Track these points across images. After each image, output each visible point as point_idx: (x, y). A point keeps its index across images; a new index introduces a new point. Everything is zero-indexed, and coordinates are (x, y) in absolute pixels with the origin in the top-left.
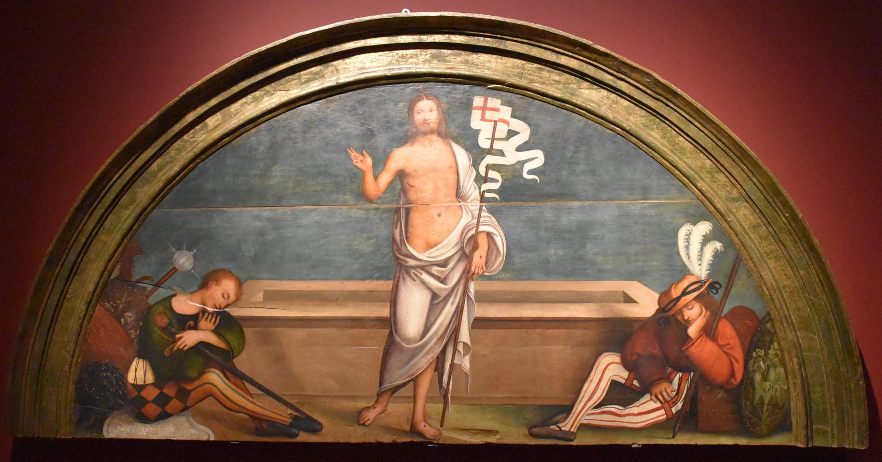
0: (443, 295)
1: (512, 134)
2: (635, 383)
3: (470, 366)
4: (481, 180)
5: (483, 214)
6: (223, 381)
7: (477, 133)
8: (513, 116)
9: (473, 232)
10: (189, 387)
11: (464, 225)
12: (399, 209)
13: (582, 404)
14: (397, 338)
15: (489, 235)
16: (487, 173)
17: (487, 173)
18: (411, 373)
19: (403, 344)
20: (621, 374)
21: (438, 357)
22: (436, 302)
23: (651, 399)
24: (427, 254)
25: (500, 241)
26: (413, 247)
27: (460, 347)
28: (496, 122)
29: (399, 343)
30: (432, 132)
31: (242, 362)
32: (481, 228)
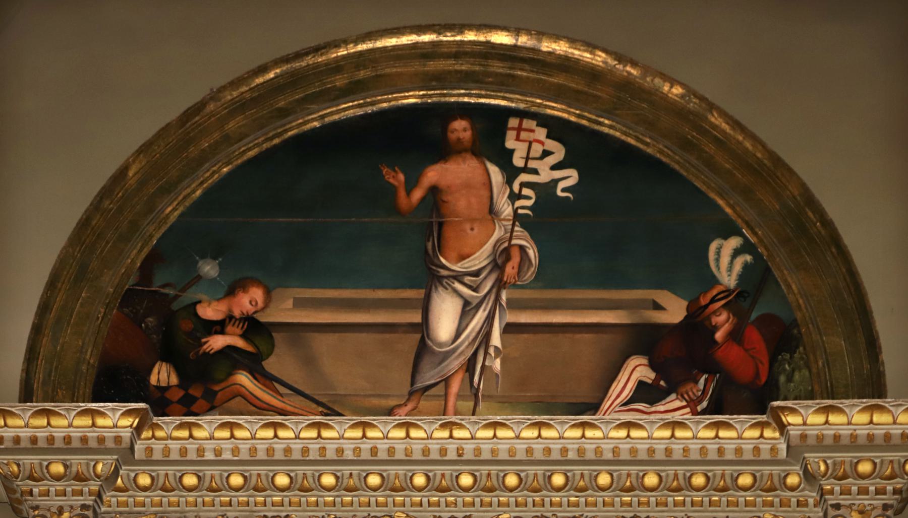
1: (546, 154)
2: (662, 383)
3: (501, 368)
5: (516, 228)
6: (252, 382)
7: (512, 152)
8: (548, 137)
9: (506, 245)
10: (216, 388)
11: (496, 239)
12: (432, 223)
13: (609, 402)
14: (429, 342)
15: (522, 248)
16: (520, 190)
17: (520, 190)
18: (442, 374)
19: (435, 347)
20: (648, 375)
21: (469, 360)
22: (468, 308)
23: (677, 399)
24: (459, 265)
25: (532, 253)
26: (445, 258)
27: (492, 351)
28: (530, 143)
29: (431, 347)
30: (465, 150)
31: (271, 365)
32: (514, 242)
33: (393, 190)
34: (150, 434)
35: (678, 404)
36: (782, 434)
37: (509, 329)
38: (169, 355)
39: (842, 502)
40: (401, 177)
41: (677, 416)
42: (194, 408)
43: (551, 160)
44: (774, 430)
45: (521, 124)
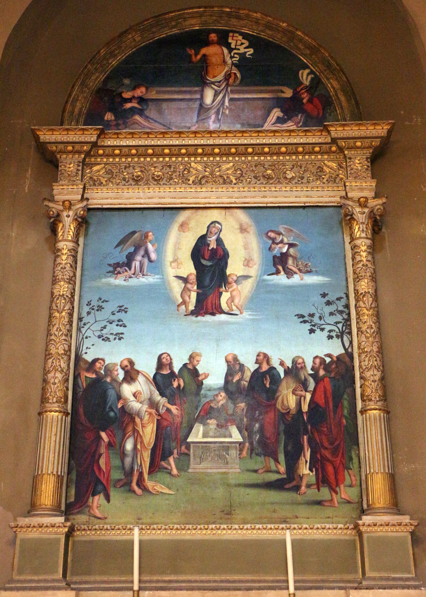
0: (219, 91)
1: (242, 44)
2: (286, 117)
4: (232, 57)
7: (230, 43)
8: (243, 38)
10: (128, 121)
15: (235, 74)
20: (281, 115)
25: (239, 75)
27: (225, 107)
30: (215, 43)
32: (232, 71)
33: (191, 56)
34: (104, 136)
35: (291, 124)
36: (329, 134)
37: (231, 100)
38: (111, 110)
39: (352, 157)
40: (193, 51)
41: (291, 128)
42: (120, 127)
43: (244, 46)
44: (326, 132)
45: (233, 35)
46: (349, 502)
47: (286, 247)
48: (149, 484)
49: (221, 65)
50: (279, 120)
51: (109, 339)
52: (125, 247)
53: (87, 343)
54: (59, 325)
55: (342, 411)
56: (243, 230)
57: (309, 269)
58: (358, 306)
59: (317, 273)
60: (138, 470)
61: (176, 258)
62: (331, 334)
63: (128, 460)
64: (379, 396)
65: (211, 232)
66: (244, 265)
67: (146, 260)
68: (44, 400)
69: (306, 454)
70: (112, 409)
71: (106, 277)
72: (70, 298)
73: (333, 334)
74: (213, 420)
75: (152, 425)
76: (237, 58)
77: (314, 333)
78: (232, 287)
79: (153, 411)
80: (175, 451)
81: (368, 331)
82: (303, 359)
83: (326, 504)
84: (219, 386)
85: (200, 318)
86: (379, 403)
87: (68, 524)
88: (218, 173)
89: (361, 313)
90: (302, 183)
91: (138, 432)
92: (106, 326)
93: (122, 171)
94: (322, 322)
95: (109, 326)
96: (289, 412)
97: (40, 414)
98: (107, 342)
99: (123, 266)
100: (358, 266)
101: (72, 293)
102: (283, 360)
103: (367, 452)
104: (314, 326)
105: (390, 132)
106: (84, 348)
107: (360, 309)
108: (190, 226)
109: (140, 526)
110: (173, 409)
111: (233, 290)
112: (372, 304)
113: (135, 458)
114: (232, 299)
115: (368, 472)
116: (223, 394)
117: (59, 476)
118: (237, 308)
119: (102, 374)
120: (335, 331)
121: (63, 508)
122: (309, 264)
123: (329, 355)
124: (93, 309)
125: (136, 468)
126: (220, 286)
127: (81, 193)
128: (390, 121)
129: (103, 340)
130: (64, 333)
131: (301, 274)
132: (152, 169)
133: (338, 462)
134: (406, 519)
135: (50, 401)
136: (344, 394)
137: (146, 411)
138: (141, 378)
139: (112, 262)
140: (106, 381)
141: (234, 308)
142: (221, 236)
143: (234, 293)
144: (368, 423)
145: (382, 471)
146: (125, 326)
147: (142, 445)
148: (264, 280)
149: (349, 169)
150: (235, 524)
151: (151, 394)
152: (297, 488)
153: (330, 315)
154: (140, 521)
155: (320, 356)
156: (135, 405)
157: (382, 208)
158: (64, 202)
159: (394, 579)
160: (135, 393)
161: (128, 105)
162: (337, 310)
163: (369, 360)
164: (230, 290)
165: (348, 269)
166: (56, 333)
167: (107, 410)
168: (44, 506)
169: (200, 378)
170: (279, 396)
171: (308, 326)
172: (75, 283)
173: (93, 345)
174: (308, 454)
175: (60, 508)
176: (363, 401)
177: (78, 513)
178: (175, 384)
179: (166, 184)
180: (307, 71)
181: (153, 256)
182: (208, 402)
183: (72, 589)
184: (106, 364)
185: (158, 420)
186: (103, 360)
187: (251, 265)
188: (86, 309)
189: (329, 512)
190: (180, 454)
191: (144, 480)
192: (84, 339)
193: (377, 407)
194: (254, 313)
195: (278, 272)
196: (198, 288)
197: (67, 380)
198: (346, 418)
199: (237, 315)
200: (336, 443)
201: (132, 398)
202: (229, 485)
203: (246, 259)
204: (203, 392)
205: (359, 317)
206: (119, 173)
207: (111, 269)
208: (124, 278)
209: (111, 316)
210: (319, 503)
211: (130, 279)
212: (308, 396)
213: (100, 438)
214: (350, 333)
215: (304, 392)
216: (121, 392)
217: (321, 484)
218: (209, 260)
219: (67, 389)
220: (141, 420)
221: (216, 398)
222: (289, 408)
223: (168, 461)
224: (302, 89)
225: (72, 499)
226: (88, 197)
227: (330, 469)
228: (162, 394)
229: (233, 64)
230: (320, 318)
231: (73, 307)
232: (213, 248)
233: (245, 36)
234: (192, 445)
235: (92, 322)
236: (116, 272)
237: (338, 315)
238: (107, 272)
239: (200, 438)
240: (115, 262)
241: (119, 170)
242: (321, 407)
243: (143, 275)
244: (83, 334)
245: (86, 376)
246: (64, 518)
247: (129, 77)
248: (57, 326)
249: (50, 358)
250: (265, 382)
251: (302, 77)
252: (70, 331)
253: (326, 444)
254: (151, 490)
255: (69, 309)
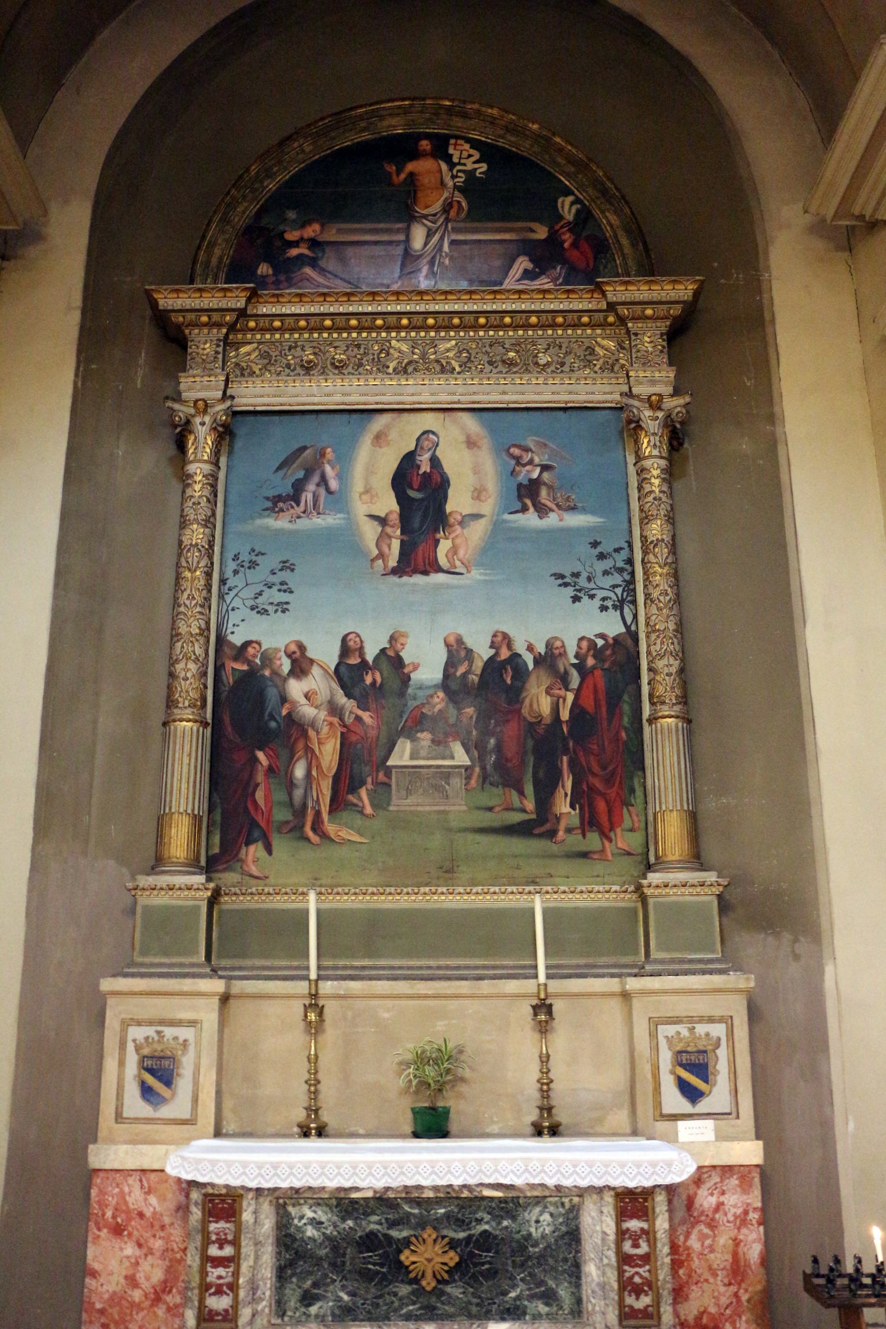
1: (470, 156)
4: (453, 177)
7: (452, 155)
15: (459, 202)
20: (530, 266)
25: (464, 204)
27: (444, 254)
33: (390, 174)
35: (546, 280)
37: (453, 243)
38: (268, 258)
40: (394, 168)
41: (546, 287)
42: (281, 286)
46: (629, 854)
47: (538, 470)
48: (330, 828)
49: (437, 188)
50: (528, 275)
51: (266, 611)
52: (290, 472)
53: (234, 618)
54: (191, 590)
55: (621, 719)
56: (471, 443)
57: (572, 505)
58: (646, 560)
59: (584, 511)
60: (313, 808)
61: (368, 487)
62: (605, 603)
63: (298, 793)
64: (677, 696)
65: (422, 448)
66: (473, 498)
67: (322, 491)
68: (170, 703)
69: (566, 784)
70: (272, 717)
71: (261, 516)
72: (207, 549)
73: (609, 603)
74: (425, 733)
75: (333, 740)
76: (462, 178)
77: (579, 601)
78: (454, 531)
79: (336, 720)
80: (369, 780)
81: (662, 598)
82: (563, 642)
83: (596, 856)
84: (435, 683)
85: (405, 579)
86: (677, 708)
87: (212, 885)
88: (432, 357)
89: (651, 571)
90: (562, 372)
91: (313, 751)
92: (262, 591)
93: (285, 354)
94: (592, 585)
95: (267, 592)
96: (541, 720)
97: (165, 724)
98: (264, 616)
99: (287, 500)
100: (646, 500)
101: (210, 541)
102: (532, 642)
103: (656, 781)
104: (579, 591)
105: (697, 294)
106: (230, 625)
107: (649, 565)
108: (390, 438)
109: (318, 889)
110: (366, 716)
111: (457, 536)
112: (667, 558)
113: (309, 792)
114: (454, 550)
115: (658, 809)
116: (441, 694)
117: (195, 816)
118: (463, 563)
119: (257, 664)
120: (610, 598)
121: (203, 862)
122: (573, 497)
123: (602, 636)
124: (242, 566)
125: (310, 805)
126: (437, 530)
127: (222, 387)
128: (697, 278)
129: (258, 612)
130: (200, 602)
131: (560, 512)
132: (332, 349)
133: (613, 795)
134: (711, 877)
135: (180, 705)
136: (623, 692)
137: (324, 721)
138: (316, 671)
139: (271, 493)
140: (263, 676)
141: (458, 563)
142: (438, 453)
143: (458, 541)
144: (659, 736)
145: (679, 808)
146: (291, 592)
147: (320, 770)
148: (505, 521)
149: (634, 350)
150: (458, 886)
151: (332, 695)
152: (551, 834)
153: (604, 575)
154: (318, 882)
155: (588, 636)
156: (308, 711)
157: (684, 411)
158: (196, 402)
159: (691, 961)
160: (308, 693)
161: (294, 252)
162: (614, 567)
163: (662, 643)
164: (453, 535)
165: (631, 505)
166: (187, 602)
167: (266, 718)
168: (175, 860)
169: (406, 671)
170: (526, 697)
171: (570, 591)
172: (215, 527)
173: (243, 620)
174: (569, 784)
175: (199, 862)
176: (652, 704)
177: (224, 870)
178: (368, 680)
179: (353, 374)
180: (571, 198)
181: (333, 484)
182: (417, 707)
183: (221, 977)
184: (263, 649)
185: (342, 734)
186: (259, 644)
187: (483, 498)
188: (231, 566)
189: (599, 867)
190: (376, 783)
191: (323, 822)
192: (230, 612)
193: (673, 713)
194: (488, 572)
195: (524, 509)
196: (402, 534)
197: (205, 674)
198: (626, 729)
199: (462, 574)
200: (610, 768)
201: (303, 701)
202: (450, 830)
203: (476, 489)
204: (410, 691)
205: (648, 578)
206: (281, 356)
207: (269, 504)
208: (289, 518)
209: (271, 576)
210: (585, 855)
211: (298, 520)
212: (570, 697)
213: (256, 760)
214: (634, 602)
215: (563, 690)
216: (287, 691)
217: (587, 828)
218: (418, 490)
219: (206, 687)
220: (318, 733)
221: (430, 700)
222: (540, 715)
223: (359, 793)
224: (562, 227)
225: (217, 850)
226: (233, 394)
227: (601, 806)
228: (348, 695)
229: (455, 186)
230: (589, 579)
231: (212, 563)
232: (425, 472)
233: (475, 144)
234: (394, 771)
235: (240, 587)
236: (277, 509)
237: (615, 573)
238: (264, 510)
239: (406, 761)
240: (276, 493)
241: (281, 352)
242: (588, 713)
243: (319, 513)
244: (228, 602)
245: (233, 668)
246: (204, 876)
247: (294, 209)
248: (188, 592)
249: (178, 641)
250: (504, 676)
251: (563, 207)
252: (208, 599)
253: (596, 769)
254: (333, 837)
255: (206, 566)
